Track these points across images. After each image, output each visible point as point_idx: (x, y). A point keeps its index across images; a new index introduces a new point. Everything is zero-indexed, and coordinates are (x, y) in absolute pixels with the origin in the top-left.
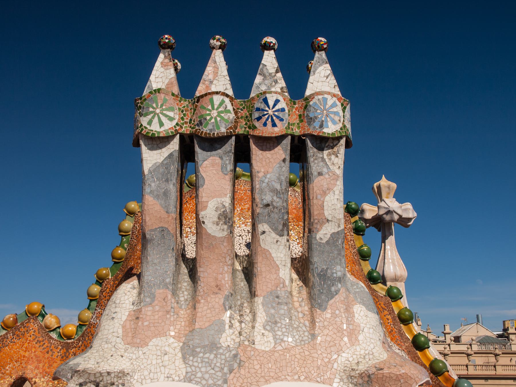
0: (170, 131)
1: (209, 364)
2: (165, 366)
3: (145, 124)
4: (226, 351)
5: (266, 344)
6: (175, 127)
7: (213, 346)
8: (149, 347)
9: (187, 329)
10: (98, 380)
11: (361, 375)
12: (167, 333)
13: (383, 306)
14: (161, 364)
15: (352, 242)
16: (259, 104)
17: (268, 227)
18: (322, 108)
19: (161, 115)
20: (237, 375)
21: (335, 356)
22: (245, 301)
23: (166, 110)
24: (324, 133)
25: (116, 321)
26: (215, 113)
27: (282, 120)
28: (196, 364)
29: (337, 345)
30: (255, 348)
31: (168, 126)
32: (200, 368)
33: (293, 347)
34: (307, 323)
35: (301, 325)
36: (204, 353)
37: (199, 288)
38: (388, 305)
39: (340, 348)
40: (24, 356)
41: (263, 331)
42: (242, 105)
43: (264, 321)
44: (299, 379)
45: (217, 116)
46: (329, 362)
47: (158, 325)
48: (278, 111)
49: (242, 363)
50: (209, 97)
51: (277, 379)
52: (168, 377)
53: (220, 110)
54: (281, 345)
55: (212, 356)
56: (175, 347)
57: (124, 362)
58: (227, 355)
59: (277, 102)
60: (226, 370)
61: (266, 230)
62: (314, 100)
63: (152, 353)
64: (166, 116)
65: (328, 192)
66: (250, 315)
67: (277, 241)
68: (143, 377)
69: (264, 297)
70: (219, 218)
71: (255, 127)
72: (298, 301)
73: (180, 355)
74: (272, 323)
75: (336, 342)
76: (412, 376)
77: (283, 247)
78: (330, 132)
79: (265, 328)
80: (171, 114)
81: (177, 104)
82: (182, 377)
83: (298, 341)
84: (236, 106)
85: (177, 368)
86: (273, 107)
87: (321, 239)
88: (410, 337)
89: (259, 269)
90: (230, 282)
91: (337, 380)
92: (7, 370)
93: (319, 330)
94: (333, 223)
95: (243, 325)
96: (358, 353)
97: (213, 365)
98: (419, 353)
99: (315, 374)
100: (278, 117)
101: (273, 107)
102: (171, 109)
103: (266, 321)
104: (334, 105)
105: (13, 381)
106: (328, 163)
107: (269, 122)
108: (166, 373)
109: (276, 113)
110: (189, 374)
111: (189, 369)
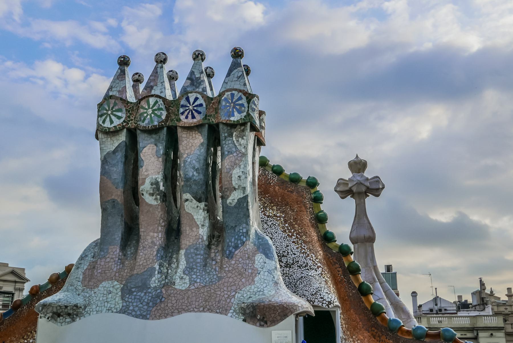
0: (118, 127)
1: (140, 300)
2: (108, 302)
3: (101, 123)
4: (153, 291)
6: (122, 123)
7: (144, 286)
8: (99, 288)
9: (129, 274)
10: (59, 312)
11: (247, 306)
12: (114, 278)
13: (335, 260)
14: (105, 301)
15: (311, 209)
16: (183, 102)
17: (190, 196)
18: (230, 101)
19: (111, 115)
20: (158, 308)
21: (234, 293)
23: (116, 111)
24: (230, 121)
25: (80, 269)
26: (150, 111)
27: (199, 113)
28: (130, 300)
29: (237, 284)
30: (174, 288)
31: (117, 122)
32: (133, 303)
33: (203, 287)
34: (217, 269)
35: (213, 270)
37: (140, 244)
38: (340, 260)
39: (238, 287)
41: (182, 275)
42: (172, 103)
43: (184, 267)
44: (203, 311)
45: (152, 113)
47: (108, 272)
48: (196, 106)
49: (163, 299)
50: (147, 99)
51: (188, 311)
52: (108, 310)
53: (154, 108)
54: (194, 285)
55: (143, 294)
56: (118, 288)
57: (79, 299)
58: (154, 293)
59: (196, 99)
60: (151, 304)
61: (189, 198)
62: (225, 96)
63: (101, 292)
64: (115, 115)
65: (235, 167)
66: (176, 264)
67: (197, 207)
68: (91, 310)
69: (186, 249)
70: (153, 190)
71: (179, 120)
73: (120, 293)
75: (236, 282)
76: (288, 307)
77: (202, 210)
78: (236, 120)
79: (184, 273)
80: (119, 114)
81: (125, 106)
82: (119, 310)
84: (167, 105)
85: (116, 303)
86: (193, 104)
87: (230, 203)
88: (357, 285)
89: (184, 228)
90: (162, 239)
91: (231, 311)
93: (225, 274)
94: (239, 190)
96: (252, 291)
97: (142, 301)
98: (363, 299)
100: (196, 111)
101: (193, 104)
102: (120, 110)
103: (186, 267)
104: (240, 98)
106: (236, 144)
107: (190, 116)
108: (109, 306)
109: (195, 108)
110: (124, 307)
111: (125, 304)
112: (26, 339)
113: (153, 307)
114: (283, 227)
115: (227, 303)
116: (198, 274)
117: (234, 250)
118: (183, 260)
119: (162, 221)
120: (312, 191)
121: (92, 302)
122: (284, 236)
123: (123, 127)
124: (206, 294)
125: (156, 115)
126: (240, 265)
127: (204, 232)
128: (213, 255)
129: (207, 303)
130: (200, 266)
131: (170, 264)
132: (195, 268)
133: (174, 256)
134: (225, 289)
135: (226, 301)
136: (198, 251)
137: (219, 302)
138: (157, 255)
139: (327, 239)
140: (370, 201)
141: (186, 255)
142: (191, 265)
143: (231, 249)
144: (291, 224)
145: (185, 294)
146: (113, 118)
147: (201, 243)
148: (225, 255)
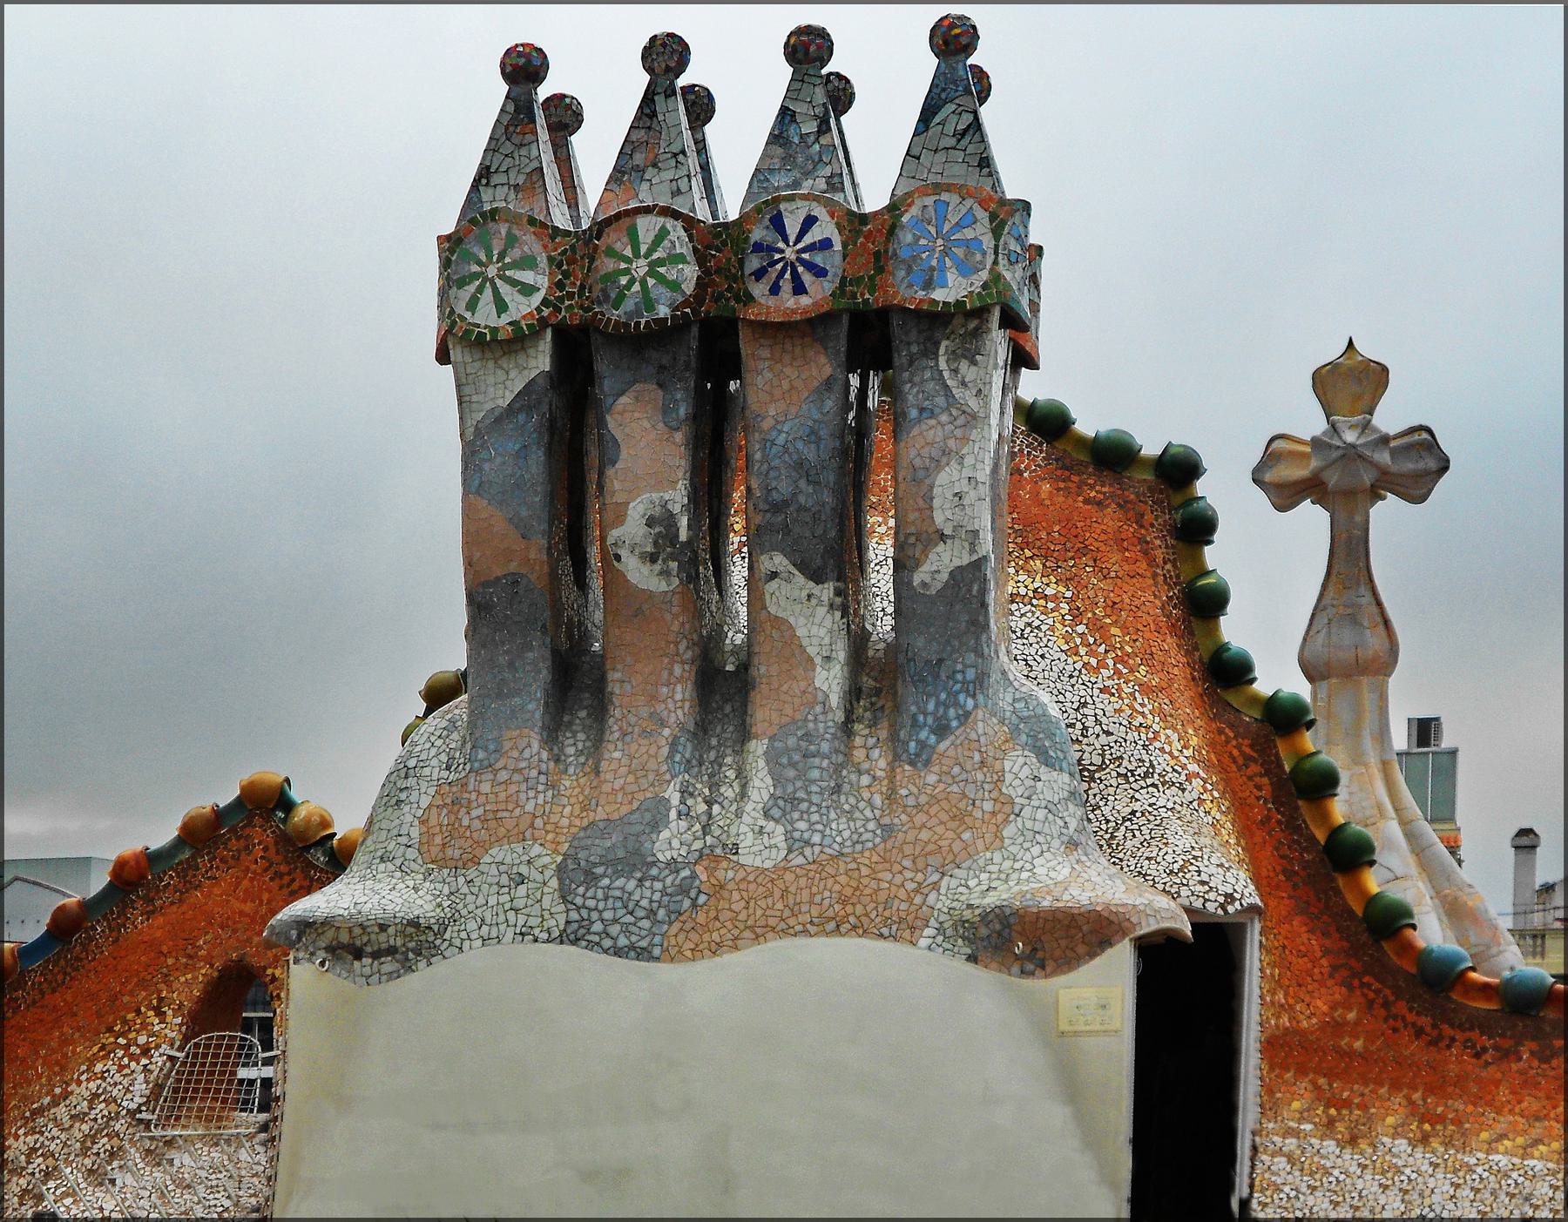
5: (766, 853)
11: (984, 917)
15: (1168, 566)
21: (936, 877)
22: (729, 751)
23: (516, 265)
34: (878, 800)
35: (862, 805)
36: (618, 874)
39: (950, 857)
40: (242, 913)
41: (762, 822)
43: (766, 798)
46: (917, 891)
51: (787, 932)
69: (772, 738)
72: (864, 746)
74: (783, 805)
79: (767, 814)
81: (545, 247)
83: (848, 843)
89: (763, 670)
90: (687, 704)
91: (928, 932)
92: (200, 948)
93: (903, 817)
95: (716, 809)
99: (878, 920)
102: (527, 263)
105: (216, 974)
112: (123, 1034)
113: (670, 924)
114: (1067, 638)
115: (913, 908)
116: (815, 817)
117: (933, 739)
118: (760, 775)
119: (684, 644)
120: (1177, 499)
121: (464, 912)
122: (1069, 668)
123: (543, 323)
124: (843, 879)
125: (662, 280)
126: (955, 788)
127: (831, 680)
128: (859, 754)
129: (849, 909)
130: (821, 793)
131: (714, 786)
132: (803, 800)
133: (728, 760)
134: (906, 863)
135: (910, 901)
136: (811, 743)
137: (887, 904)
138: (670, 756)
139: (1226, 672)
140: (1388, 517)
141: (772, 758)
142: (790, 789)
143: (923, 735)
144: (1096, 627)
145: (772, 881)
146: (504, 289)
147: (821, 718)
148: (904, 757)
